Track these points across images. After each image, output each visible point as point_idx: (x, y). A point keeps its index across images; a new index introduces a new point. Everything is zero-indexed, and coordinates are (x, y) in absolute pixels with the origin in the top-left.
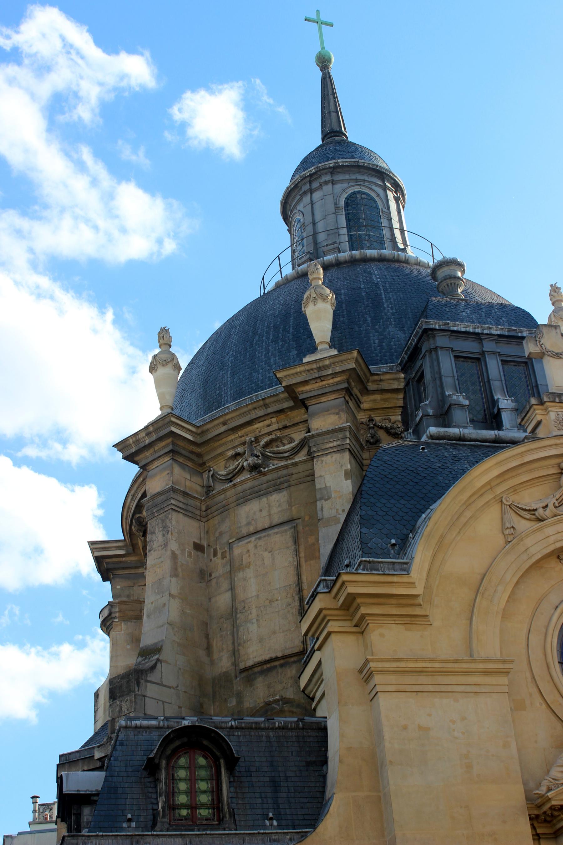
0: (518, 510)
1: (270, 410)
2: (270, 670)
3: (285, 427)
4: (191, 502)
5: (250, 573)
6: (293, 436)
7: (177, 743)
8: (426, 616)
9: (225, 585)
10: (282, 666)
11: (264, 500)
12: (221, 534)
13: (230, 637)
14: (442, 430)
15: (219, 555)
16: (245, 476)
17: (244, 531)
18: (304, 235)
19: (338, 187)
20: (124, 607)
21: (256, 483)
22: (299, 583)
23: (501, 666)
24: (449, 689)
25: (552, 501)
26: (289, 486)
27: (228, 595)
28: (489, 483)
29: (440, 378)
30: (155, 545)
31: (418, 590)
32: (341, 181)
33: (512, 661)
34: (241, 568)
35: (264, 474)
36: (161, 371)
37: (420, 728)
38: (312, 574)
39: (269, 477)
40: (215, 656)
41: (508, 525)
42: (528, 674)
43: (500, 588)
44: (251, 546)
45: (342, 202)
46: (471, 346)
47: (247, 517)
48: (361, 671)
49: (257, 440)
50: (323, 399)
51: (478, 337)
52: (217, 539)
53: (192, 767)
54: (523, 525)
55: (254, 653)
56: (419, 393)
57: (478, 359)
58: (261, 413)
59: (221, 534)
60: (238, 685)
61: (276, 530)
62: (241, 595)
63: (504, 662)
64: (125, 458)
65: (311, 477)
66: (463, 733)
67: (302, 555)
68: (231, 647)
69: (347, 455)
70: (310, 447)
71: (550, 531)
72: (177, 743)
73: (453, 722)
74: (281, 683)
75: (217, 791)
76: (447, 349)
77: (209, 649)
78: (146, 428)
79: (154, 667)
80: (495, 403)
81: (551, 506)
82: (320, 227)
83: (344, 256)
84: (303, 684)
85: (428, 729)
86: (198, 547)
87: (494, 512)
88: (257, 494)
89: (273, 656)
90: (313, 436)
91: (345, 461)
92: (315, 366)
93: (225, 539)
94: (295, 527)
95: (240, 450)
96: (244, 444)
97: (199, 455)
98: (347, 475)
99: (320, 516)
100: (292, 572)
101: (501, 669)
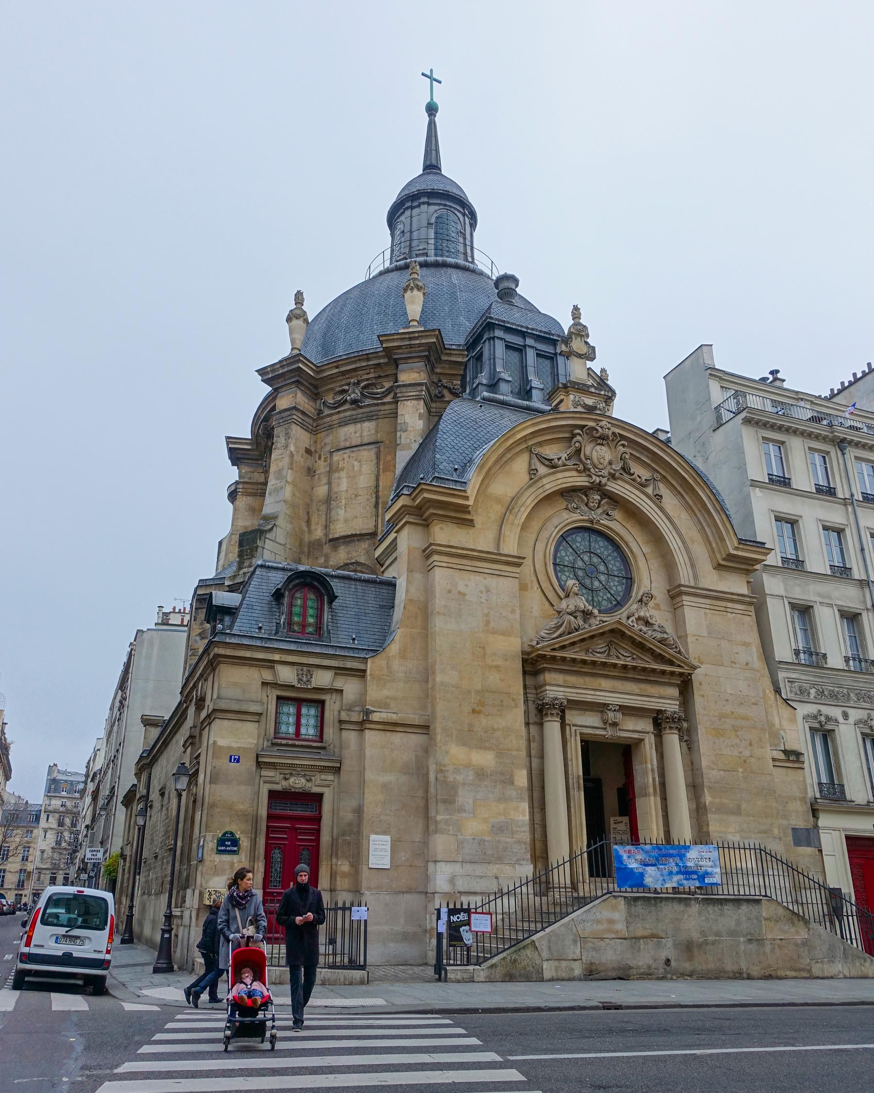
0: (543, 459)
1: (371, 363)
2: (350, 542)
3: (380, 377)
4: (306, 419)
5: (343, 474)
6: (384, 384)
7: (297, 581)
8: (472, 521)
9: (324, 480)
10: (358, 540)
11: (359, 425)
12: (325, 444)
13: (324, 516)
14: (492, 395)
16: (347, 406)
17: (342, 445)
18: (403, 240)
19: (432, 208)
20: (246, 486)
21: (354, 413)
22: (377, 486)
23: (516, 560)
24: (481, 570)
25: (564, 456)
27: (326, 487)
28: (524, 437)
29: (494, 359)
30: (279, 445)
31: (470, 502)
32: (435, 204)
33: (524, 558)
34: (338, 470)
35: (361, 407)
36: (295, 322)
37: (460, 593)
38: (387, 481)
40: (313, 527)
41: (533, 467)
42: (532, 568)
43: (522, 509)
44: (346, 456)
45: (433, 220)
46: (517, 340)
47: (346, 435)
48: (424, 551)
49: (359, 382)
51: (523, 334)
53: (305, 600)
54: (543, 470)
55: (340, 529)
56: (477, 367)
57: (520, 350)
58: (364, 364)
59: (325, 444)
60: (327, 549)
61: (364, 447)
62: (335, 489)
63: (519, 558)
64: (263, 381)
65: (395, 415)
66: (487, 600)
67: (381, 467)
68: (324, 523)
69: (422, 402)
70: (396, 394)
71: (560, 475)
72: (297, 581)
73: (481, 592)
74: (357, 551)
75: (319, 617)
76: (501, 339)
77: (308, 522)
78: (280, 362)
79: (272, 529)
80: (528, 382)
81: (563, 458)
82: (415, 235)
83: (432, 259)
84: (377, 555)
85: (464, 595)
86: (308, 451)
87: (525, 457)
88: (354, 421)
89: (354, 533)
90: (399, 386)
91: (421, 406)
92: (407, 336)
94: (379, 448)
95: (346, 387)
96: (349, 384)
97: (316, 387)
98: (421, 416)
99: (398, 442)
100: (373, 477)
101: (516, 562)
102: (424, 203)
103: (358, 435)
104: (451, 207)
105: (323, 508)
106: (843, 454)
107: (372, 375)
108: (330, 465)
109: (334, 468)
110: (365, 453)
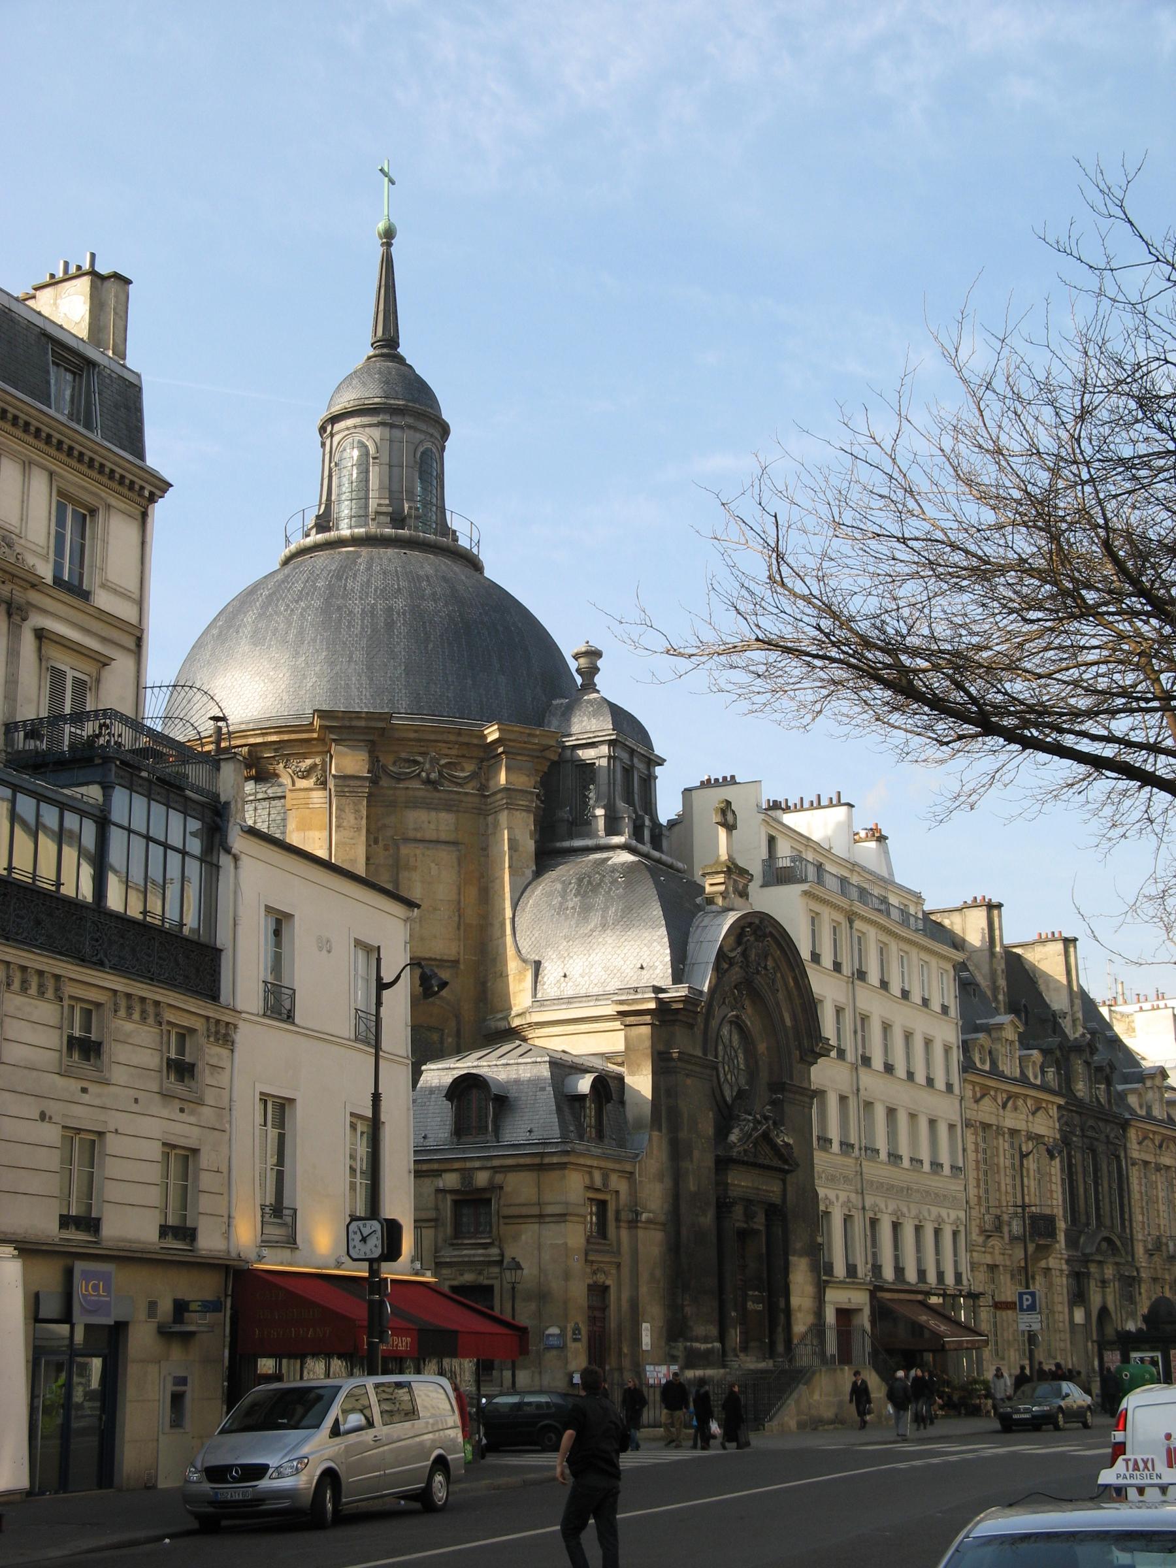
3: (463, 756)
5: (416, 876)
6: (465, 765)
11: (433, 814)
15: (381, 844)
16: (416, 784)
17: (411, 834)
19: (419, 436)
22: (459, 902)
26: (458, 811)
35: (438, 791)
39: (442, 795)
44: (418, 852)
50: (519, 758)
51: (632, 752)
58: (452, 738)
59: (385, 826)
61: (443, 847)
88: (429, 806)
89: (433, 956)
93: (389, 833)
95: (420, 759)
103: (432, 826)
106: (851, 928)
107: (454, 752)
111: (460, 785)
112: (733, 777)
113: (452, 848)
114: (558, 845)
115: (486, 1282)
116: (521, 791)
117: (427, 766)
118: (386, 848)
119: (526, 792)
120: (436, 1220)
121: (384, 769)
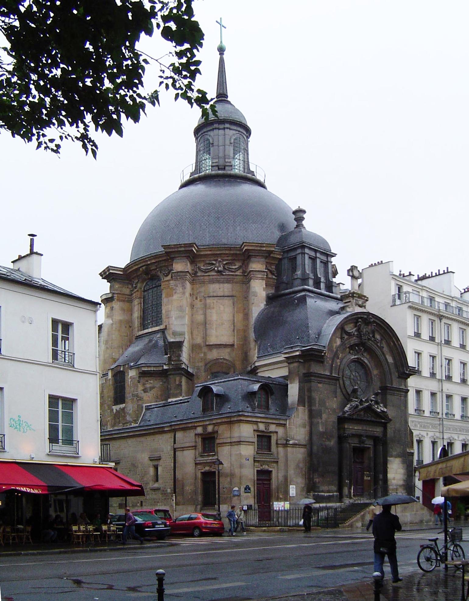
5: (214, 311)
9: (201, 312)
11: (222, 285)
12: (200, 292)
17: (211, 294)
21: (219, 277)
22: (234, 320)
35: (223, 275)
44: (215, 301)
45: (232, 141)
52: (198, 293)
58: (227, 252)
59: (200, 292)
62: (209, 318)
88: (219, 282)
95: (214, 262)
102: (227, 128)
103: (221, 290)
104: (242, 132)
105: (201, 328)
107: (230, 258)
108: (205, 305)
109: (208, 306)
110: (227, 301)
111: (232, 272)
112: (382, 261)
113: (230, 298)
114: (279, 293)
115: (213, 470)
116: (258, 271)
117: (217, 265)
118: (201, 301)
119: (261, 271)
120: (195, 446)
121: (199, 268)
